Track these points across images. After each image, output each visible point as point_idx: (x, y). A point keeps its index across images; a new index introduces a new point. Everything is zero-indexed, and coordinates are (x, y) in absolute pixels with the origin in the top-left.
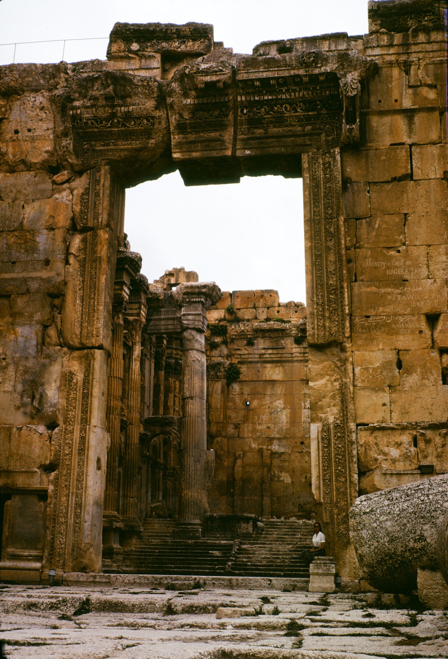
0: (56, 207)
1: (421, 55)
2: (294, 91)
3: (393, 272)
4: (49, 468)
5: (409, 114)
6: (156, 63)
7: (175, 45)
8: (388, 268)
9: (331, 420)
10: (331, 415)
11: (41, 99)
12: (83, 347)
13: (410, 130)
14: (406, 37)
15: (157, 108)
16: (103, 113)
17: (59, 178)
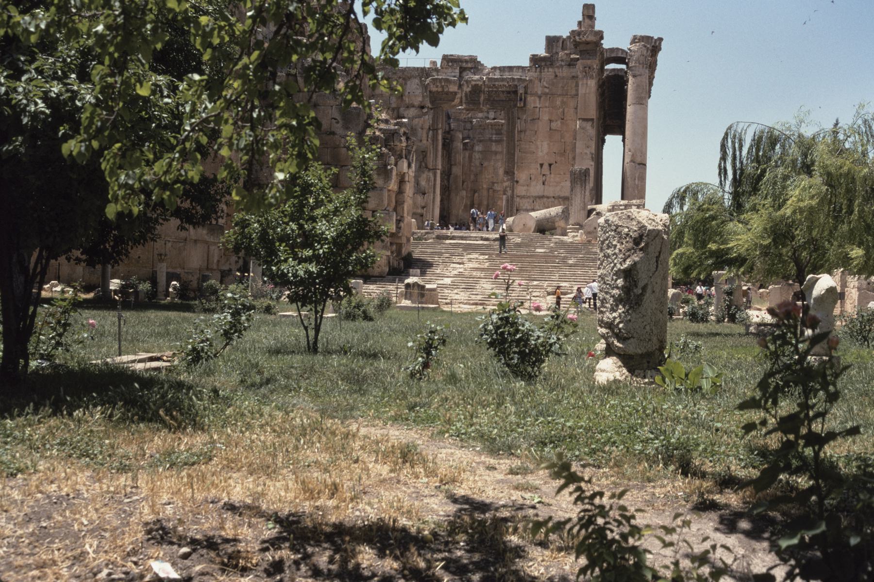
0: (424, 121)
4: (423, 208)
5: (540, 97)
6: (457, 71)
7: (464, 65)
10: (509, 193)
16: (440, 89)
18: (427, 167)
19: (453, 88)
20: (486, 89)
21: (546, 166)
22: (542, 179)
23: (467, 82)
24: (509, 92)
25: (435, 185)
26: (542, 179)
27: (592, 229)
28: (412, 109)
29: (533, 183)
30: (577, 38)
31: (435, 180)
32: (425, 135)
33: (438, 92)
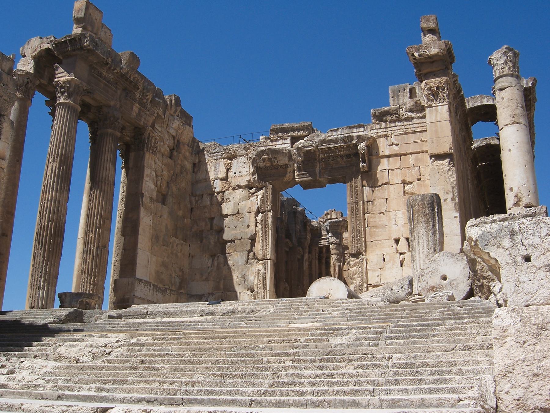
1: (393, 132)
2: (342, 151)
3: (382, 222)
6: (289, 141)
8: (380, 221)
9: (358, 283)
11: (244, 159)
12: (263, 259)
13: (389, 164)
14: (386, 124)
15: (289, 161)
16: (268, 164)
17: (252, 191)
18: (255, 258)
19: (283, 161)
20: (321, 156)
21: (403, 242)
22: (399, 258)
23: (298, 149)
24: (348, 156)
25: (265, 279)
26: (399, 258)
27: (436, 280)
28: (239, 191)
29: (388, 265)
30: (416, 54)
31: (265, 273)
32: (253, 219)
33: (266, 168)
